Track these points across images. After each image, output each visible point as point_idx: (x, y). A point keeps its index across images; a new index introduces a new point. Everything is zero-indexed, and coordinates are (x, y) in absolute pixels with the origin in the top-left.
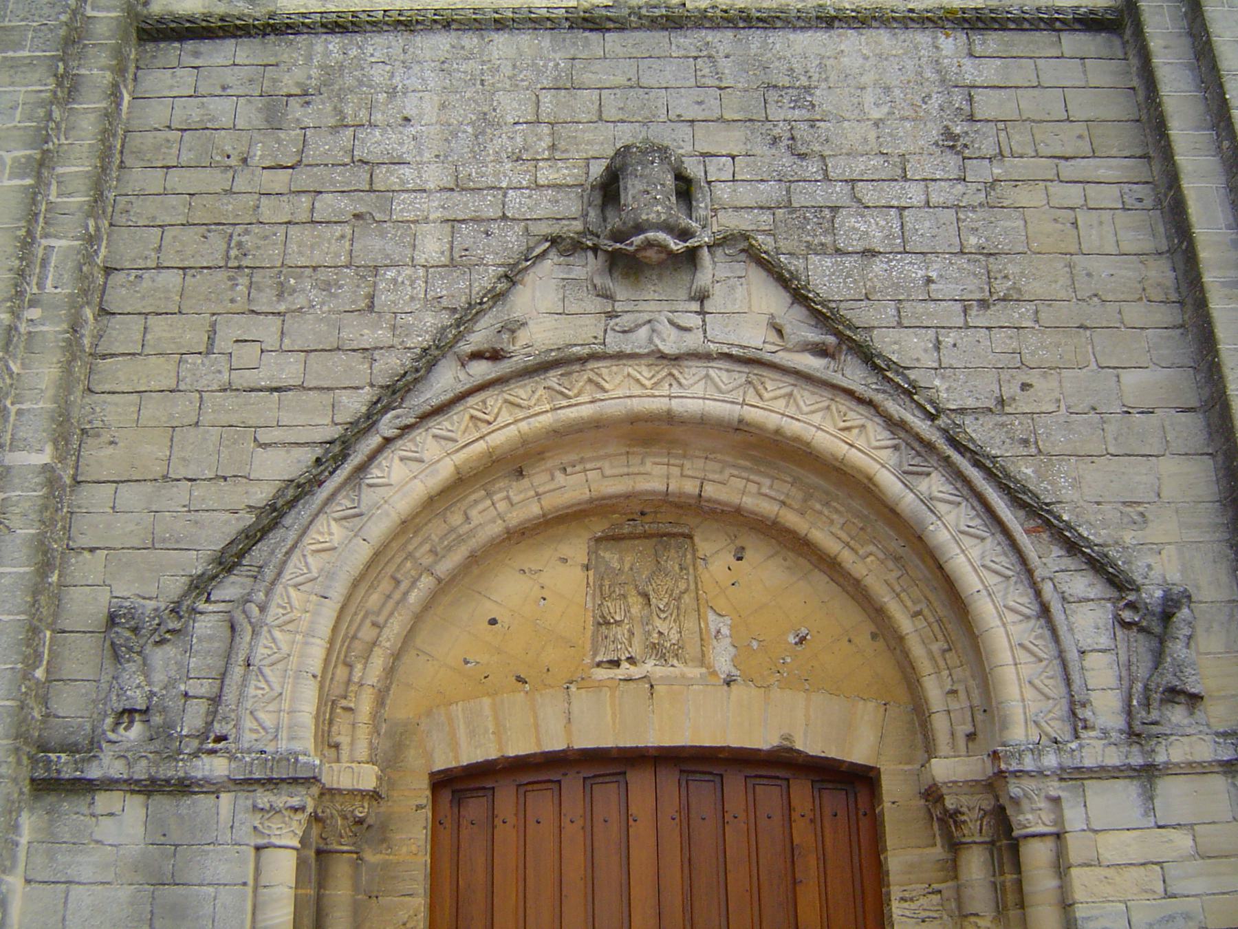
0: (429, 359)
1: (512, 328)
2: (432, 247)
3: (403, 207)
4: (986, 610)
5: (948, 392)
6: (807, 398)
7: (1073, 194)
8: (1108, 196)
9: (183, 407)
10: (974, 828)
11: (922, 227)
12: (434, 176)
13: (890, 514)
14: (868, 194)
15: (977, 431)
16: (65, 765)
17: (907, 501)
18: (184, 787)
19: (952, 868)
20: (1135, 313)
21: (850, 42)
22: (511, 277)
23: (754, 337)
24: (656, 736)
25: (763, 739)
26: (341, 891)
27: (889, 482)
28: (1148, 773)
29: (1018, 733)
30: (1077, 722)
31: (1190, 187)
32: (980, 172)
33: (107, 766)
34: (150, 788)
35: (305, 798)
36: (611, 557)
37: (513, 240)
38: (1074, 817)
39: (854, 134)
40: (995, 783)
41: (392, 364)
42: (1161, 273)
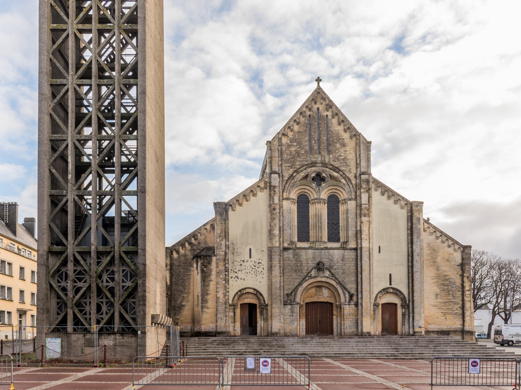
0: (307, 276)
1: (311, 275)
2: (306, 268)
3: (303, 265)
4: (341, 294)
5: (340, 280)
6: (331, 280)
7: (350, 264)
8: (353, 264)
9: (290, 280)
10: (339, 307)
11: (339, 267)
12: (306, 262)
13: (335, 287)
14: (336, 264)
15: (341, 282)
16: (285, 303)
17: (337, 287)
18: (293, 304)
19: (337, 309)
20: (353, 274)
21: (336, 251)
22: (311, 270)
23: (327, 275)
24: (319, 301)
25: (326, 301)
26: (301, 310)
27: (335, 286)
28: (349, 305)
29: (342, 302)
30: (346, 301)
31: (358, 265)
32: (344, 263)
33: (288, 303)
34: (290, 304)
35: (299, 305)
36: (317, 289)
37: (311, 268)
38: (345, 307)
39: (335, 259)
40: (340, 305)
41: (303, 277)
42: (356, 271)
